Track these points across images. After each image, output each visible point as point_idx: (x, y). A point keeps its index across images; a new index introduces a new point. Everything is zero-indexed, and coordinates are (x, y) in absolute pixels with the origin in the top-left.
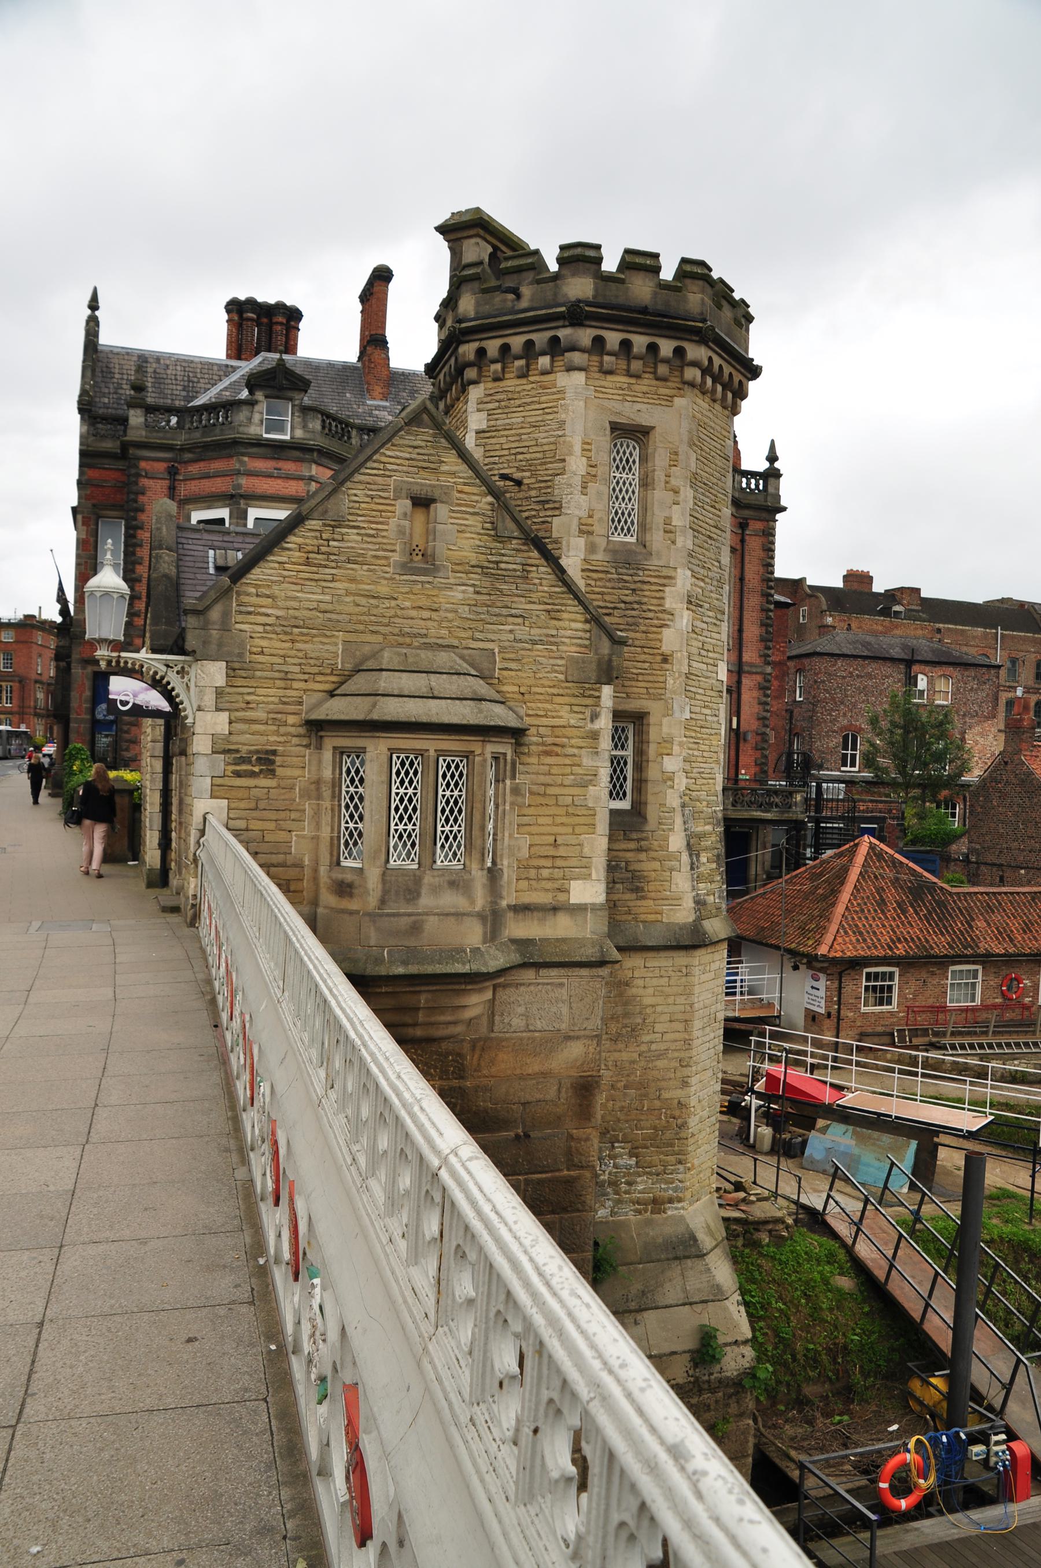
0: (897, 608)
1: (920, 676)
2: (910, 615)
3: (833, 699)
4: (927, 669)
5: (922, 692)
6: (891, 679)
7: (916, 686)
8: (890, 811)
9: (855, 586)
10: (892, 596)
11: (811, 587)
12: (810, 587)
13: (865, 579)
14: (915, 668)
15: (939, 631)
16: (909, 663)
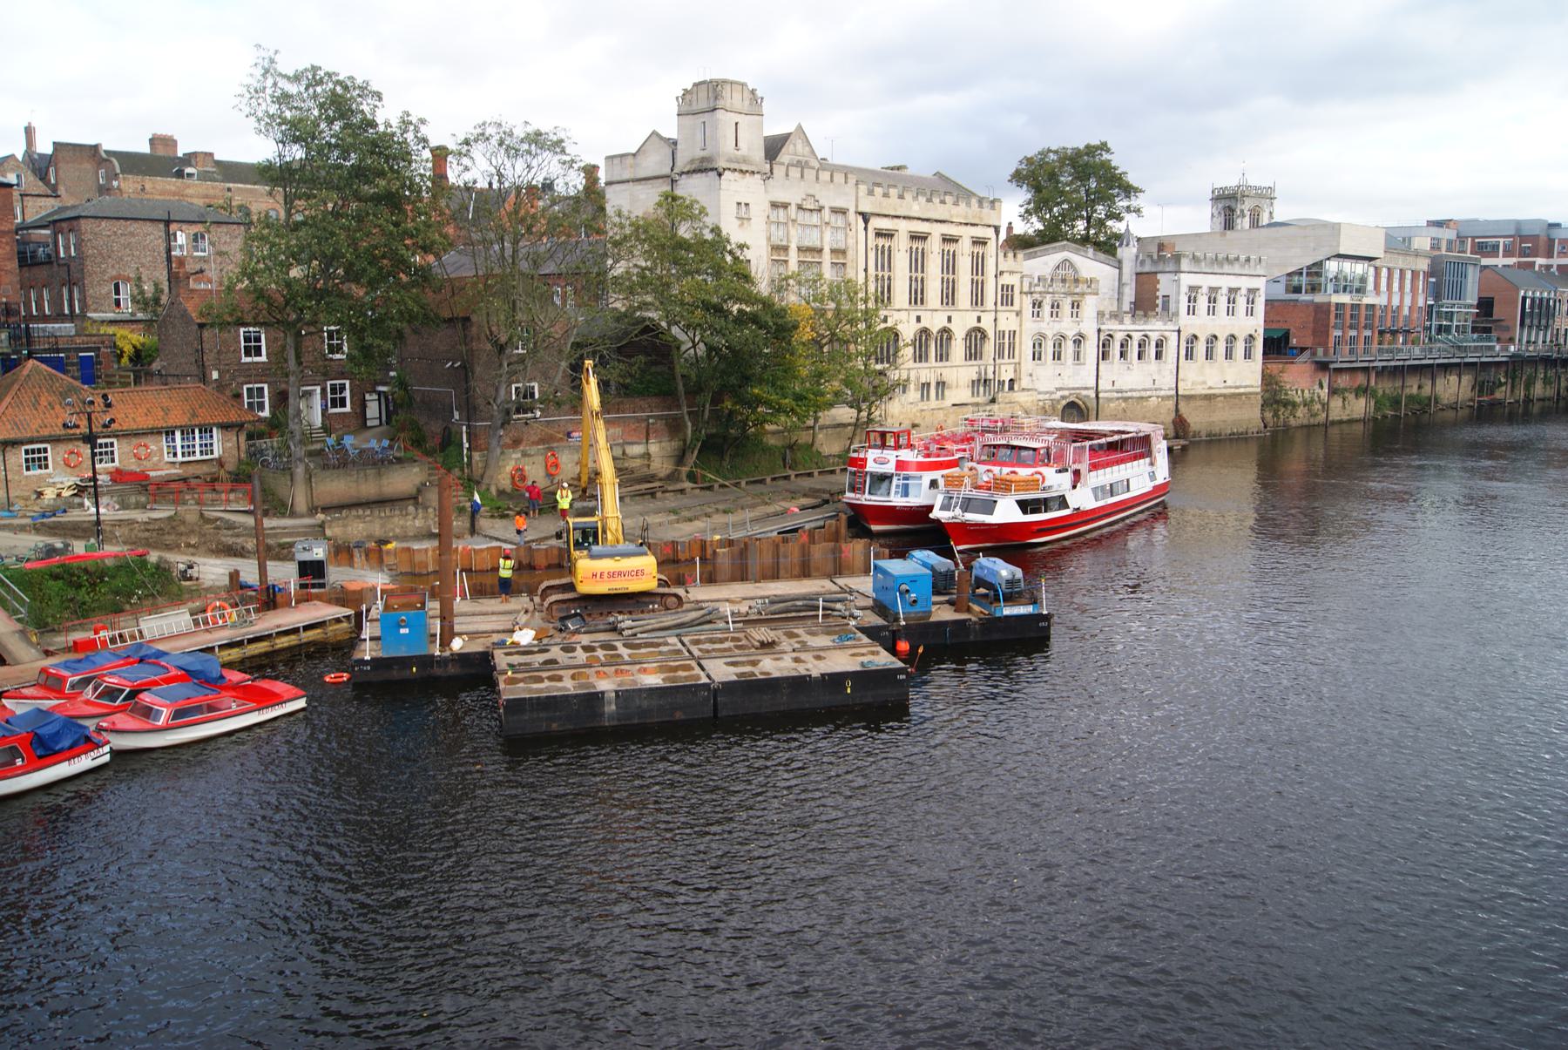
0: (189, 170)
1: (179, 233)
2: (204, 177)
3: (101, 254)
4: (184, 227)
5: (181, 247)
6: (155, 233)
7: (175, 240)
8: (103, 342)
9: (161, 152)
10: (190, 158)
11: (107, 152)
12: (105, 152)
13: (169, 142)
14: (173, 227)
15: (229, 190)
16: (168, 223)
